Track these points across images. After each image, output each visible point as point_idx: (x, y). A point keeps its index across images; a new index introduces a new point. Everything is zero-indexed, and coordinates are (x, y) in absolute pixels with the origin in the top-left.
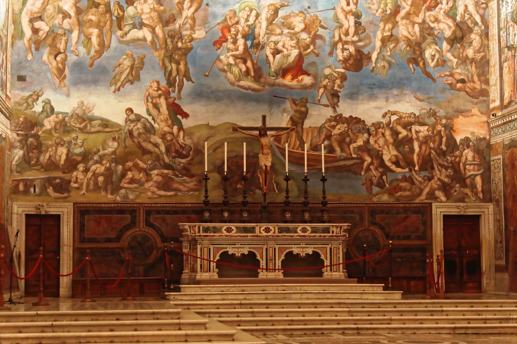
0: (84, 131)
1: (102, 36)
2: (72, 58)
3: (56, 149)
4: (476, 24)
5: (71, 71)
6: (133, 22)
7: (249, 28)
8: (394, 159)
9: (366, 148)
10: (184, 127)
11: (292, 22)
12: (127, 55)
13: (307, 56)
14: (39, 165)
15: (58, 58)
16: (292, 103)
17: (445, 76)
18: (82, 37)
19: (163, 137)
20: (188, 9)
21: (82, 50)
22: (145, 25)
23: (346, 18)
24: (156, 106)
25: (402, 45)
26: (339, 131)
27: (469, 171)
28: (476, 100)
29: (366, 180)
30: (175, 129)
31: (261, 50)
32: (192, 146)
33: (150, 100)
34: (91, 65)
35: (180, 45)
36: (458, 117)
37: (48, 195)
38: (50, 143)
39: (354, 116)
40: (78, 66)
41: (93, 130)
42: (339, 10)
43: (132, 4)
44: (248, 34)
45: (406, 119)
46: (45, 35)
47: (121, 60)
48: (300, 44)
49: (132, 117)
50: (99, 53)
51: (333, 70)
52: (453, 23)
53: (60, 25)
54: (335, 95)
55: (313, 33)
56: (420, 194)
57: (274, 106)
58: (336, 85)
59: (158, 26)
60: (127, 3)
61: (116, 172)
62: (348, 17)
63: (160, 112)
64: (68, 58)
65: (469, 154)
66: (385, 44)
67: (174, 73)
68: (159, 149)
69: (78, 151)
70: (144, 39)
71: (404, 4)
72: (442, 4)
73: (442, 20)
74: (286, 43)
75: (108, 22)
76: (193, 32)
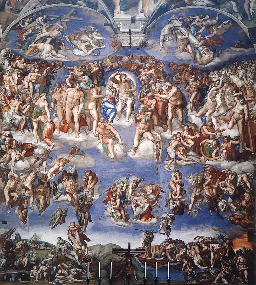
0: (36, 249)
1: (45, 199)
2: (30, 211)
3: (22, 259)
4: (247, 187)
5: (30, 219)
6: (61, 191)
7: (123, 193)
8: (200, 262)
9: (185, 256)
10: (88, 246)
11: (146, 189)
12: (58, 209)
13: (153, 208)
14: (14, 267)
15: (23, 212)
16: (145, 233)
17: (230, 216)
18: (35, 200)
19: (77, 252)
20: (90, 184)
21: (35, 207)
22: (68, 193)
23: (175, 186)
24: (73, 236)
25: (206, 200)
26: (171, 247)
27: (241, 267)
28: (246, 229)
29: (184, 273)
30: (83, 247)
31: (129, 205)
32: (92, 256)
33: (70, 232)
34: (40, 215)
35: (86, 203)
36: (235, 238)
37: (19, 282)
38: (19, 255)
39: (178, 239)
40: (33, 215)
41: (41, 248)
42: (171, 182)
43: (61, 183)
44: (122, 196)
45: (207, 240)
46: (16, 199)
47: (55, 212)
48: (150, 201)
49: (61, 241)
50: (44, 208)
51: (167, 215)
52: (234, 187)
53: (24, 194)
54: (168, 228)
55: (157, 195)
56: (214, 280)
57: (135, 235)
58: (169, 223)
59: (74, 193)
60: (58, 182)
61: (53, 270)
62: (176, 185)
63: (75, 239)
64: (28, 211)
65: (241, 259)
66: (196, 200)
67: (82, 219)
68: (75, 258)
69: (33, 259)
70: (68, 200)
71: (208, 178)
72: (229, 177)
73: (228, 186)
74: (143, 201)
75: (49, 192)
76: (93, 196)
